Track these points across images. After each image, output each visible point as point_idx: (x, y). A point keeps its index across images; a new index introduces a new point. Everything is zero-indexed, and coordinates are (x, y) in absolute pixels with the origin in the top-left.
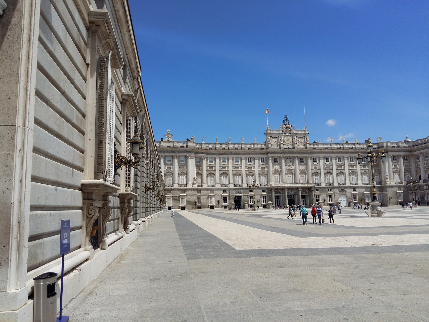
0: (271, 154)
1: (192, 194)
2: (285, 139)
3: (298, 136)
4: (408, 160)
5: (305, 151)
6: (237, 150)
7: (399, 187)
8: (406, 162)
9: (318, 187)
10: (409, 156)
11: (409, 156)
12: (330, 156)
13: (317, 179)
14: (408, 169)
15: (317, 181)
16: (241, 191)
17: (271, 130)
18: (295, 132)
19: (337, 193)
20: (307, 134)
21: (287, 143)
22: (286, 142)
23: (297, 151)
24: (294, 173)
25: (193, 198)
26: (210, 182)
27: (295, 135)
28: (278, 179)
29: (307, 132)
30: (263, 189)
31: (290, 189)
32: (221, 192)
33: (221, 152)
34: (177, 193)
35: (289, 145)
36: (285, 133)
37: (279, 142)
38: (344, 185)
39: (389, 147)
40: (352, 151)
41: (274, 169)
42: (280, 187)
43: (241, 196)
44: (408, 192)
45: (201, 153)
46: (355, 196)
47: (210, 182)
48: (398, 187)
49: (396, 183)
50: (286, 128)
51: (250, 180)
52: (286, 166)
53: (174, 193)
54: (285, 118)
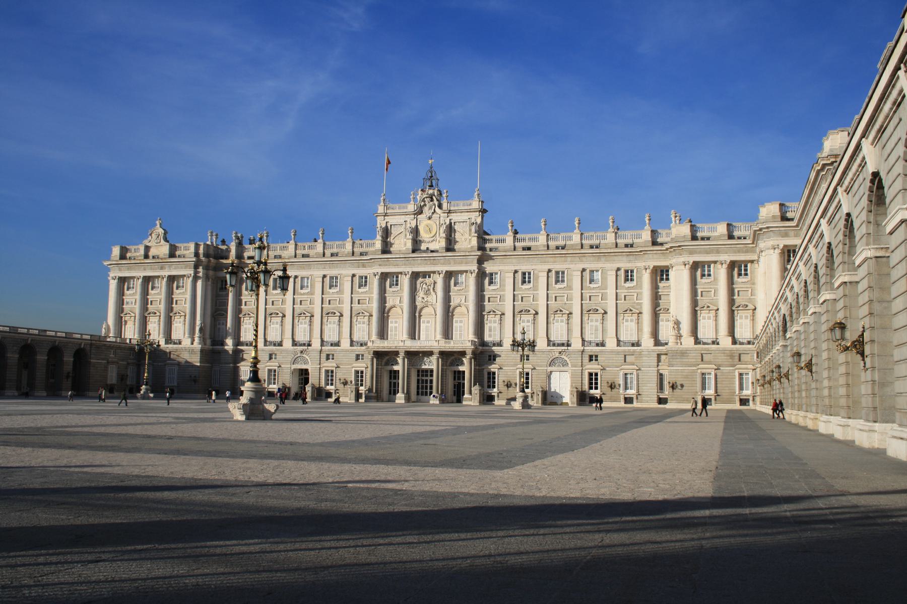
0: (380, 265)
2: (423, 222)
3: (455, 217)
6: (307, 259)
7: (705, 352)
12: (534, 267)
13: (495, 328)
16: (307, 357)
20: (477, 211)
21: (428, 236)
27: (446, 214)
30: (357, 353)
35: (432, 241)
36: (421, 212)
37: (406, 235)
38: (563, 345)
44: (731, 368)
48: (703, 352)
50: (424, 198)
51: (330, 329)
54: (430, 175)
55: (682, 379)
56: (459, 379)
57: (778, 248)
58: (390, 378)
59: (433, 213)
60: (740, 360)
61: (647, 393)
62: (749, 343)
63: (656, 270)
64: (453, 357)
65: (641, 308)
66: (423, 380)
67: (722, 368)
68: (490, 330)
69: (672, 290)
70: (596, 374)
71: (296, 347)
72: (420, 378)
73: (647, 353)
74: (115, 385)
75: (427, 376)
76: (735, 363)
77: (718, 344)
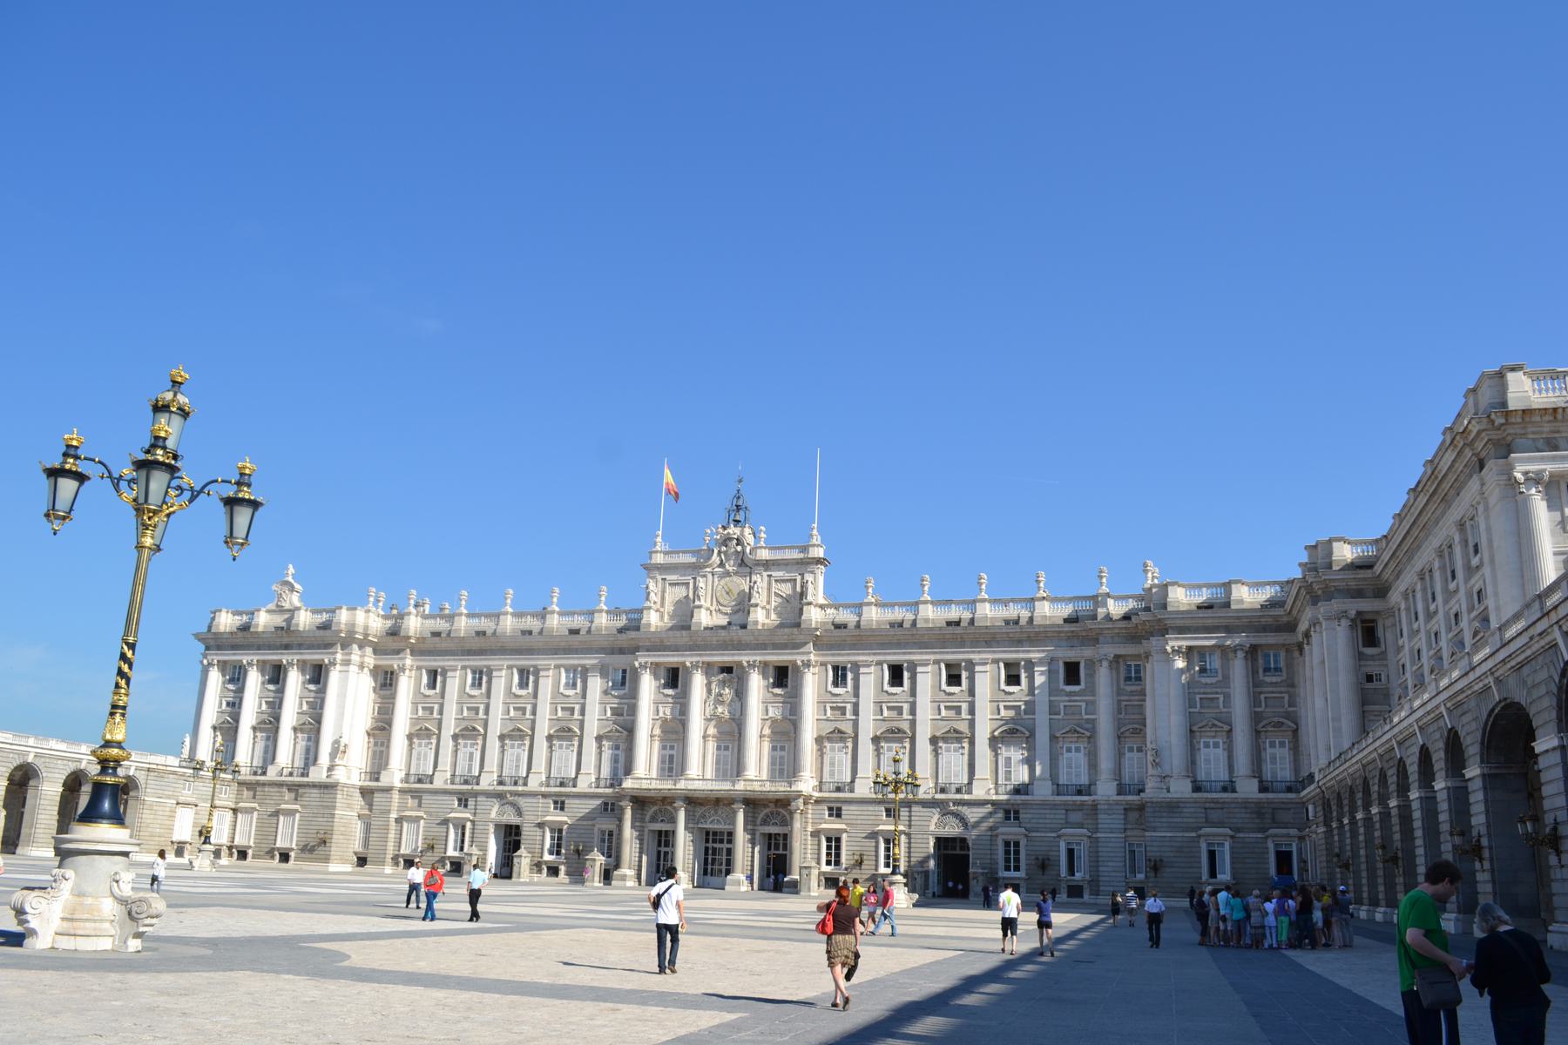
0: (648, 650)
1: (320, 804)
4: (1281, 671)
5: (786, 637)
7: (1212, 805)
8: (1271, 683)
9: (838, 800)
10: (1288, 649)
11: (1287, 651)
13: (840, 761)
14: (1276, 719)
15: (840, 772)
17: (666, 553)
18: (764, 554)
19: (925, 829)
22: (721, 601)
23: (752, 638)
24: (740, 734)
25: (320, 819)
26: (418, 765)
28: (671, 757)
29: (819, 552)
31: (694, 802)
32: (445, 806)
33: (467, 646)
34: (274, 798)
38: (958, 791)
39: (1169, 609)
40: (1011, 636)
41: (657, 717)
42: (652, 794)
43: (518, 827)
45: (394, 650)
46: (1012, 848)
47: (418, 765)
48: (1207, 805)
49: (1197, 788)
51: (560, 758)
52: (707, 705)
53: (264, 797)
55: (1172, 854)
56: (777, 847)
57: (1347, 617)
58: (659, 845)
59: (740, 565)
60: (1273, 819)
61: (1107, 879)
62: (1289, 790)
63: (1118, 662)
64: (767, 811)
65: (1094, 728)
66: (714, 850)
67: (1241, 835)
68: (832, 764)
69: (1148, 699)
70: (1017, 844)
71: (501, 788)
72: (710, 845)
73: (1106, 807)
74: (185, 843)
75: (721, 841)
76: (1267, 826)
77: (1234, 791)
